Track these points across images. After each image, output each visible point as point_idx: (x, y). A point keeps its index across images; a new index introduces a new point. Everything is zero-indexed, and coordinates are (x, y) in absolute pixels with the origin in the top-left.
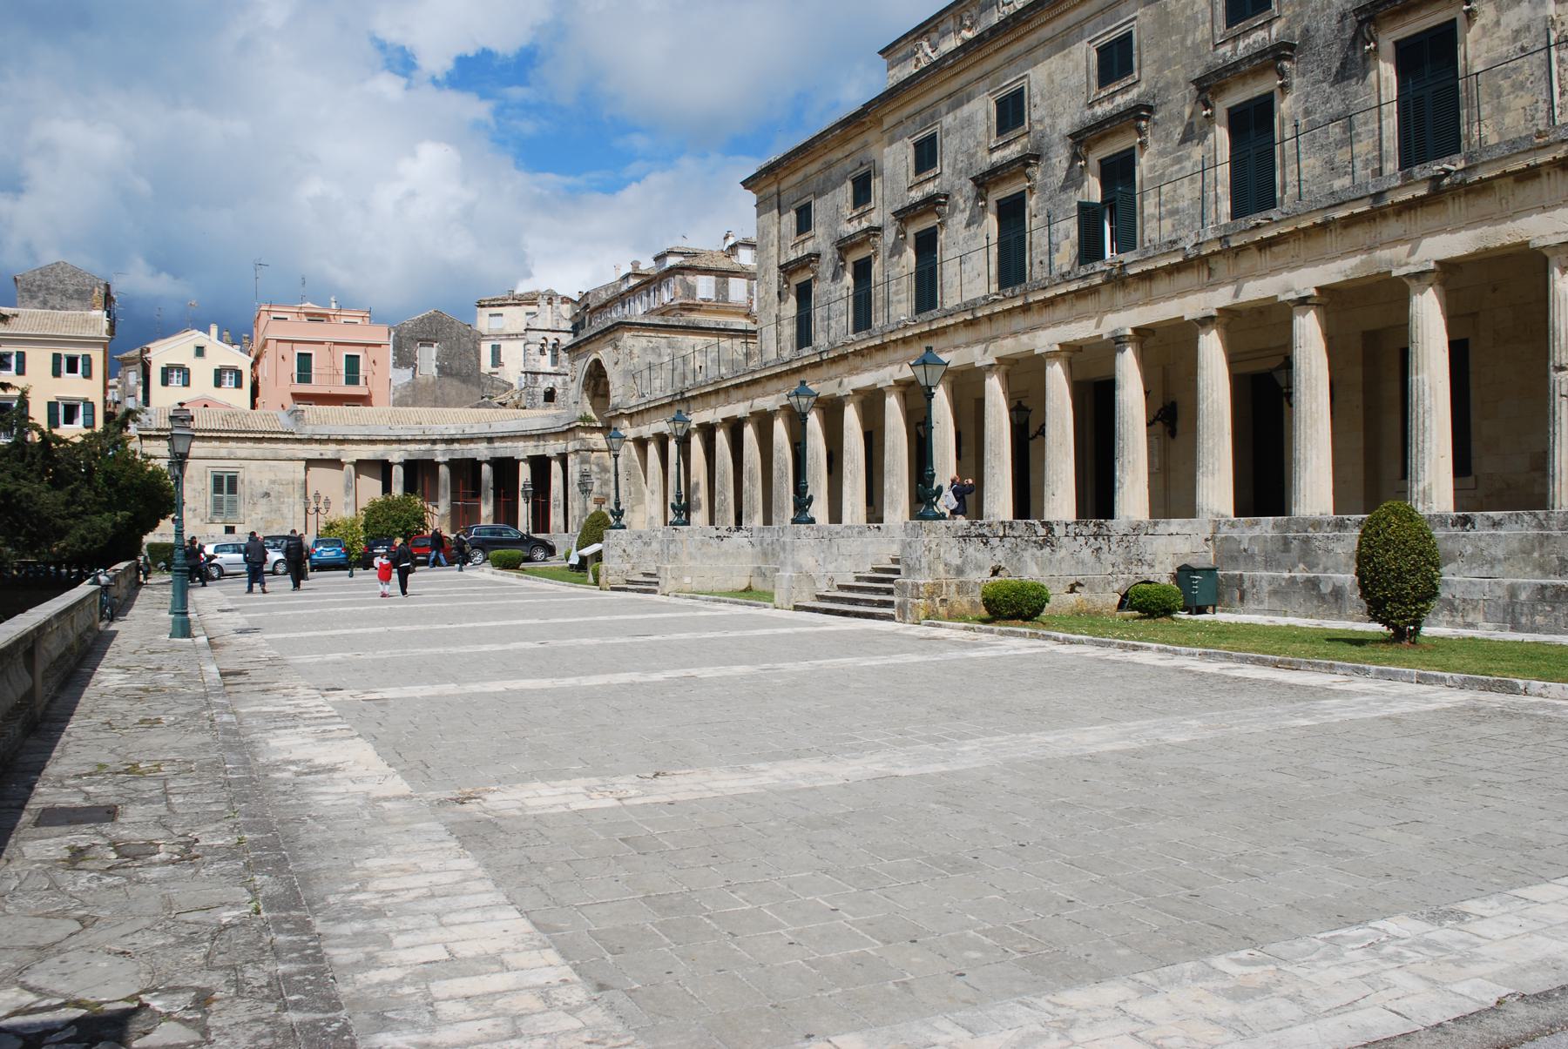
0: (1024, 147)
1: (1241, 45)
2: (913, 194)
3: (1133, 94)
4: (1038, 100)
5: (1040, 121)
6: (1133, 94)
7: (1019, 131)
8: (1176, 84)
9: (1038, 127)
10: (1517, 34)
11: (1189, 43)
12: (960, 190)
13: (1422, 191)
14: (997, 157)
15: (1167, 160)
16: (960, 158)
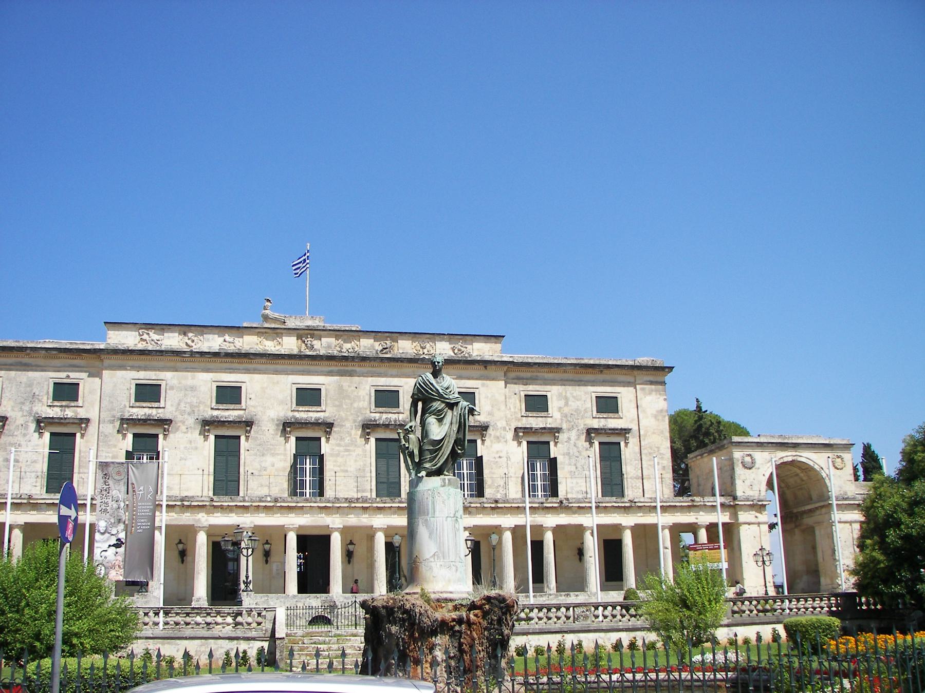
0: (239, 416)
1: (384, 416)
2: (135, 410)
3: (321, 415)
4: (252, 396)
5: (254, 407)
6: (321, 415)
7: (238, 406)
8: (347, 419)
9: (253, 409)
10: (497, 452)
11: (355, 405)
12: (183, 422)
13: (556, 505)
14: (216, 413)
15: (342, 449)
16: (183, 405)
